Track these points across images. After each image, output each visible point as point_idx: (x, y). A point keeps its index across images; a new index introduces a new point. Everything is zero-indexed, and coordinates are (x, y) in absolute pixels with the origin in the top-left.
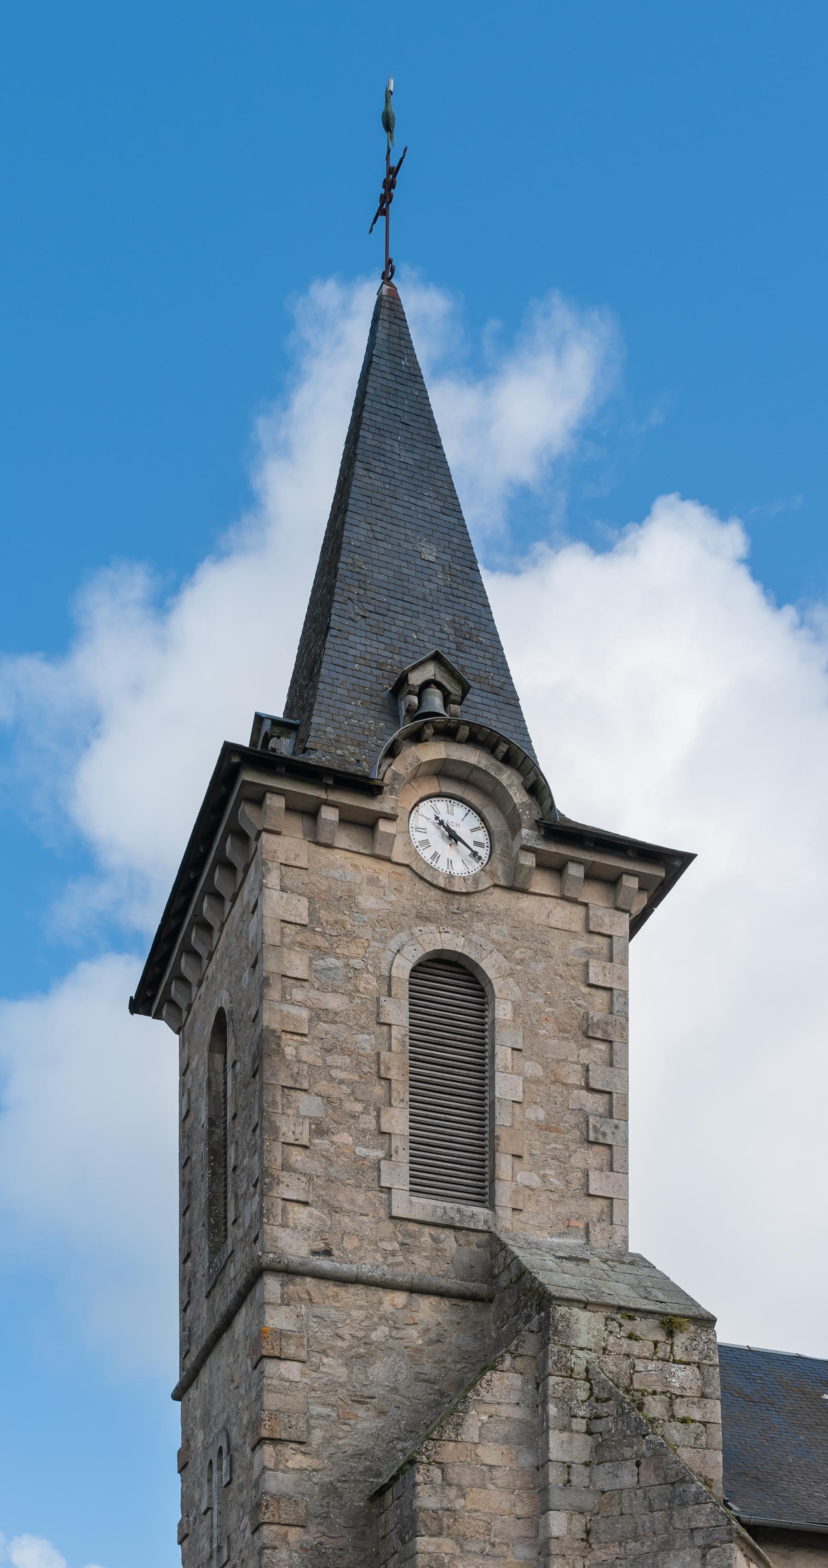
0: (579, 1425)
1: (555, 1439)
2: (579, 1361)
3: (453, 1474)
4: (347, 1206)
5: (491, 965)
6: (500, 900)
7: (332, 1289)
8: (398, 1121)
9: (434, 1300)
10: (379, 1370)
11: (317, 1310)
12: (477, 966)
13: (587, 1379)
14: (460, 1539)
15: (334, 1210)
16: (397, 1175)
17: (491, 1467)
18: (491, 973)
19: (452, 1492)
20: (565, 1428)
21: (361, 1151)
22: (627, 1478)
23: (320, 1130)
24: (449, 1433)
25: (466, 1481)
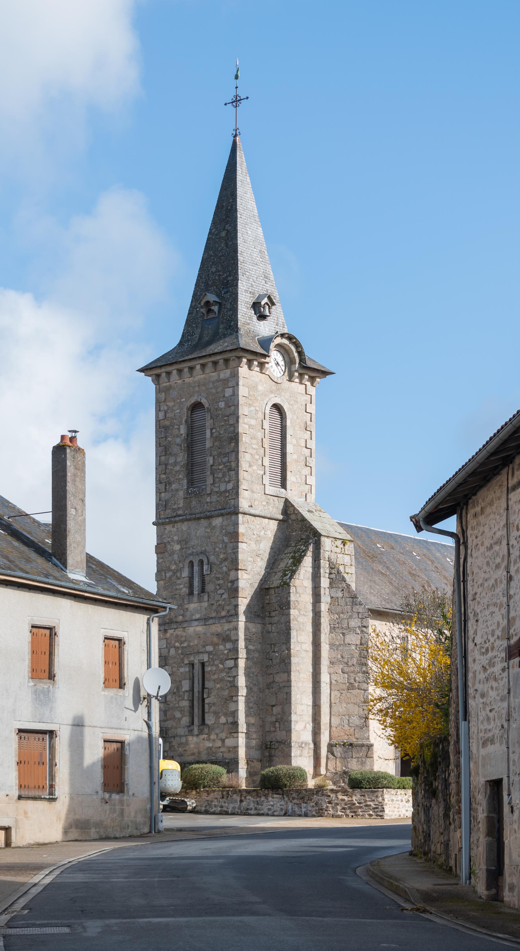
0: (327, 575)
1: (322, 579)
2: (327, 554)
3: (298, 590)
4: (255, 490)
5: (286, 407)
6: (286, 384)
7: (253, 518)
8: (267, 462)
9: (274, 521)
10: (262, 546)
11: (250, 526)
12: (283, 407)
13: (329, 561)
14: (299, 610)
15: (253, 492)
16: (266, 481)
17: (306, 587)
18: (286, 410)
19: (298, 595)
20: (324, 577)
21: (259, 472)
22: (340, 594)
23: (250, 466)
24: (297, 577)
25: (301, 592)
